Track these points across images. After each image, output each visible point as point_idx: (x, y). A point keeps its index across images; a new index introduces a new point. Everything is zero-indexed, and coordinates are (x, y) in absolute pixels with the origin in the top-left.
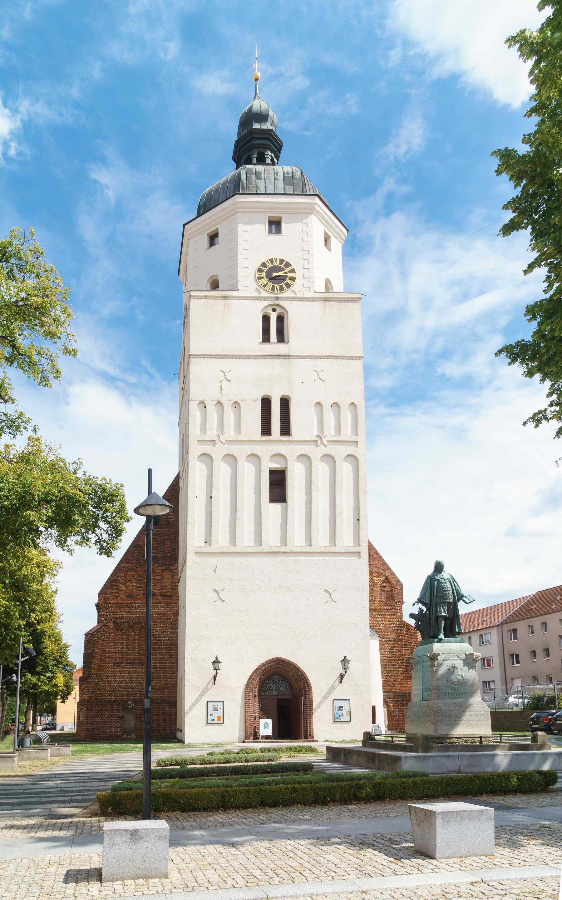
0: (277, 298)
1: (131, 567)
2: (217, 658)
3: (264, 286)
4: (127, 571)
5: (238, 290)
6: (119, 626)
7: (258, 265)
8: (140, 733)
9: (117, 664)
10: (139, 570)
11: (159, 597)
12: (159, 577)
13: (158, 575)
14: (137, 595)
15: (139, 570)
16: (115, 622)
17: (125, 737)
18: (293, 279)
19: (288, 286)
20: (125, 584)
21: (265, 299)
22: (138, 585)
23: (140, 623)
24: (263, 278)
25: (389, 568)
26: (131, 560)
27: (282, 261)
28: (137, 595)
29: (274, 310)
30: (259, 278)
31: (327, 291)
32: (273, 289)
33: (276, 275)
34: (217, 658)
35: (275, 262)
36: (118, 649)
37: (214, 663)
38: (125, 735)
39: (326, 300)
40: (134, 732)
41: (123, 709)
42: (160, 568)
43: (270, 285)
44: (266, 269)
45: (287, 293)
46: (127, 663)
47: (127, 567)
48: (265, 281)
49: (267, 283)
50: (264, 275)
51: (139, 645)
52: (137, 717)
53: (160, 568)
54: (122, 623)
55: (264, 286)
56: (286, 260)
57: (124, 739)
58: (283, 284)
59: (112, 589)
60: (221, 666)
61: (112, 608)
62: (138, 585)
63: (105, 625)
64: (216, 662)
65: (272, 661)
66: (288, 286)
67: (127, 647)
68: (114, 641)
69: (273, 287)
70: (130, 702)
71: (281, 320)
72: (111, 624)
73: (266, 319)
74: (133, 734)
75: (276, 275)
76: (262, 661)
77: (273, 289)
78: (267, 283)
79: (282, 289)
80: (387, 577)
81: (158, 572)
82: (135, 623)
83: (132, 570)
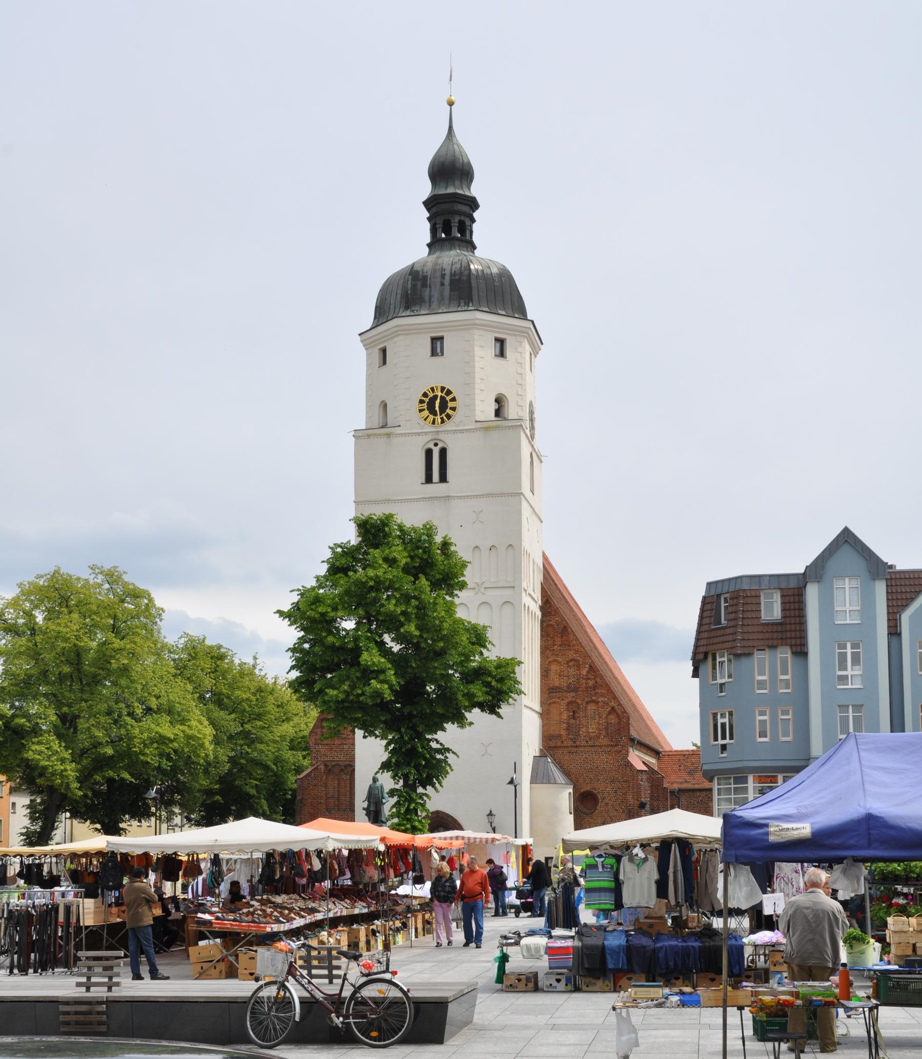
7: (420, 396)
19: (449, 417)
21: (426, 433)
25: (615, 698)
27: (443, 389)
29: (436, 445)
30: (421, 411)
32: (434, 423)
44: (427, 400)
48: (426, 413)
50: (425, 407)
55: (425, 420)
56: (447, 387)
71: (443, 452)
75: (438, 405)
77: (434, 423)
80: (613, 708)
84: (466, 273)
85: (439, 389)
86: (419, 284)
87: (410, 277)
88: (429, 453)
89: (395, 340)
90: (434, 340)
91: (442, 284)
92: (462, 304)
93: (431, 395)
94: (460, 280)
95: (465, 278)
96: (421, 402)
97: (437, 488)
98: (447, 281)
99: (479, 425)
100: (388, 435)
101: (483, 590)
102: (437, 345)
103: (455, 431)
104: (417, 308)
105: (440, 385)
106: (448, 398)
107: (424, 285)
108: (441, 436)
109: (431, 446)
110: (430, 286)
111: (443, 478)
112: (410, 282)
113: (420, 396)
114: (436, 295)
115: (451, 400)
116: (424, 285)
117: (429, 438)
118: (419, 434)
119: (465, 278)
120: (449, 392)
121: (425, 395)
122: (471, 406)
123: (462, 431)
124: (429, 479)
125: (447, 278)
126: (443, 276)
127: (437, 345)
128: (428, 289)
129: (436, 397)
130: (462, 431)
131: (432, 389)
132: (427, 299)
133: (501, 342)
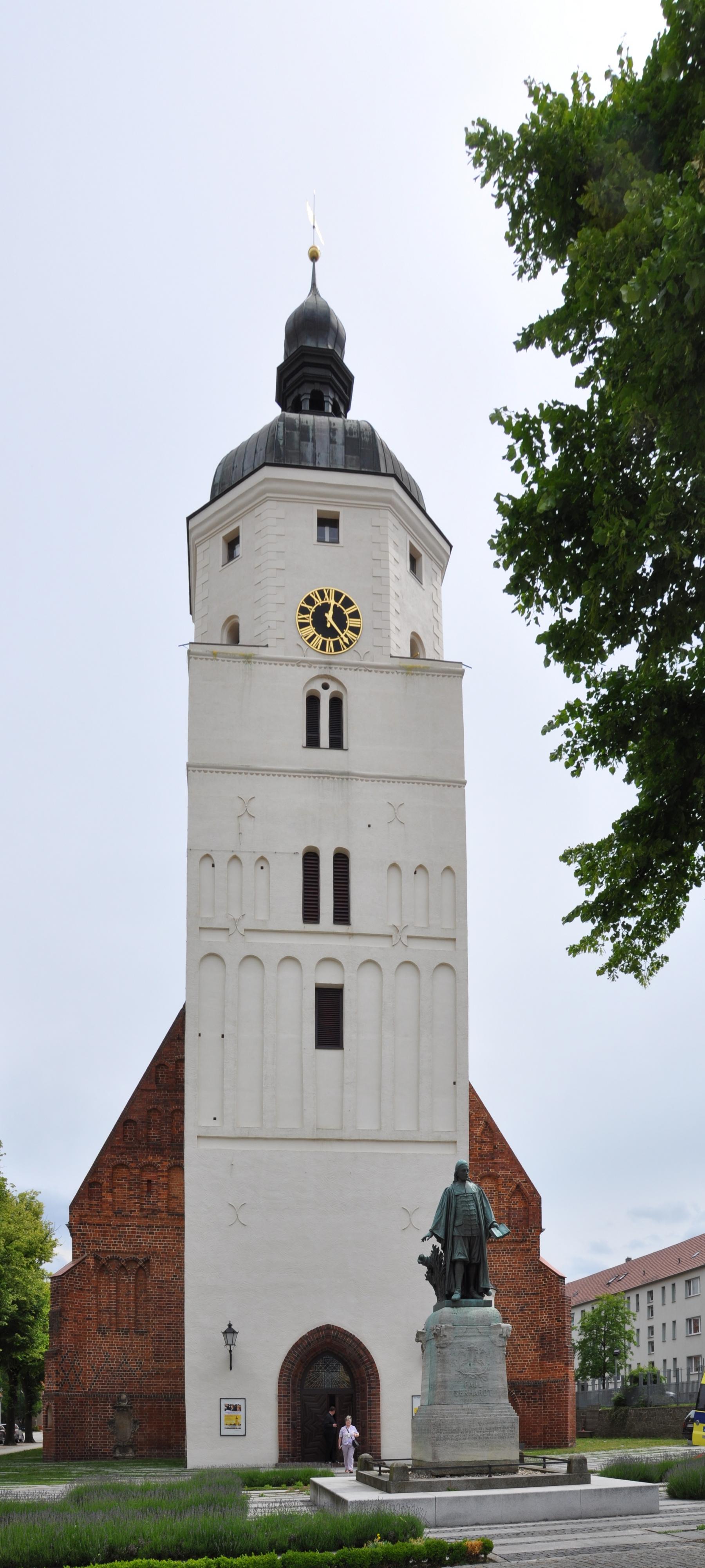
0: (329, 663)
1: (119, 1160)
2: (230, 1325)
3: (310, 641)
4: (114, 1167)
6: (103, 1265)
8: (142, 1450)
9: (102, 1331)
10: (134, 1165)
11: (164, 1215)
13: (163, 1176)
14: (131, 1211)
15: (134, 1165)
16: (97, 1259)
17: (118, 1454)
20: (111, 1191)
22: (132, 1193)
23: (136, 1261)
24: (307, 624)
26: (119, 1147)
27: (338, 596)
28: (131, 1211)
32: (323, 647)
33: (329, 619)
34: (230, 1325)
35: (326, 596)
36: (103, 1306)
37: (225, 1333)
38: (117, 1451)
40: (131, 1446)
41: (115, 1408)
42: (166, 1164)
43: (319, 638)
44: (312, 609)
46: (118, 1330)
47: (113, 1160)
48: (311, 630)
49: (314, 636)
50: (310, 621)
51: (136, 1298)
52: (135, 1422)
53: (166, 1164)
54: (108, 1260)
55: (310, 641)
57: (116, 1458)
59: (90, 1199)
60: (239, 1339)
61: (92, 1233)
62: (132, 1193)
63: (81, 1263)
64: (230, 1331)
65: (318, 1330)
67: (117, 1301)
68: (96, 1291)
69: (324, 643)
70: (124, 1396)
72: (91, 1261)
73: (313, 701)
74: (131, 1451)
76: (303, 1332)
77: (323, 647)
78: (314, 636)
81: (162, 1171)
82: (128, 1261)
83: (122, 1165)
85: (332, 595)
89: (257, 511)
91: (332, 441)
93: (319, 602)
99: (396, 662)
100: (248, 658)
101: (404, 940)
103: (357, 667)
105: (333, 589)
106: (347, 612)
108: (336, 673)
109: (317, 686)
110: (314, 441)
113: (301, 602)
117: (315, 672)
118: (298, 663)
120: (348, 603)
121: (309, 600)
122: (383, 631)
123: (368, 668)
124: (313, 741)
129: (326, 607)
130: (368, 668)
131: (321, 593)
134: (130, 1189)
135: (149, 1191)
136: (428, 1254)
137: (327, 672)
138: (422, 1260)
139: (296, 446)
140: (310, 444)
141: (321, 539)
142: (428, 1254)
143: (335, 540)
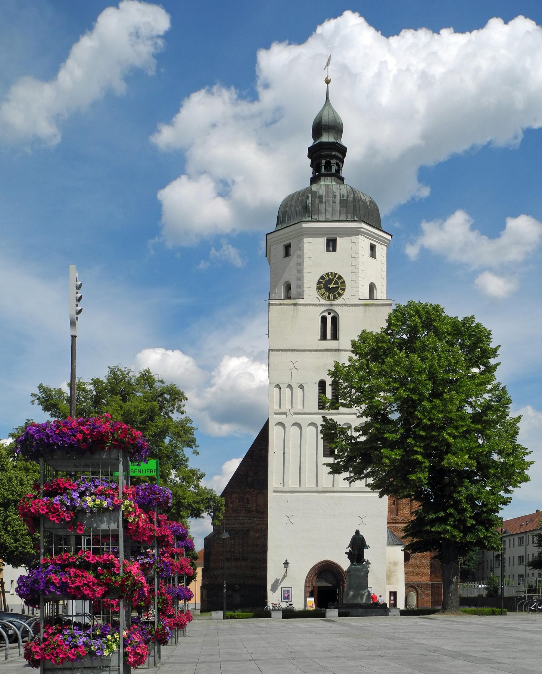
0: (331, 305)
5: (303, 298)
7: (317, 278)
12: (255, 498)
18: (344, 289)
21: (322, 305)
29: (329, 314)
31: (371, 297)
32: (328, 298)
33: (332, 286)
39: (366, 305)
42: (256, 492)
45: (339, 301)
48: (323, 291)
50: (323, 287)
53: (256, 492)
55: (322, 295)
58: (336, 293)
66: (340, 295)
69: (329, 295)
71: (335, 320)
75: (332, 286)
77: (328, 298)
79: (335, 298)
84: (352, 196)
86: (317, 201)
87: (310, 195)
88: (324, 320)
90: (328, 241)
91: (334, 202)
92: (349, 217)
93: (327, 278)
94: (347, 200)
95: (351, 199)
96: (319, 282)
97: (330, 344)
98: (338, 201)
102: (332, 245)
104: (316, 217)
107: (321, 202)
109: (326, 314)
111: (335, 337)
112: (310, 199)
114: (330, 209)
115: (341, 283)
116: (321, 202)
119: (351, 199)
125: (338, 198)
126: (334, 196)
127: (332, 245)
128: (324, 204)
131: (328, 274)
132: (323, 211)
133: (373, 248)
134: (239, 502)
135: (248, 503)
136: (348, 551)
137: (331, 308)
138: (346, 553)
139: (317, 206)
140: (324, 204)
141: (328, 250)
142: (348, 551)
143: (334, 250)
